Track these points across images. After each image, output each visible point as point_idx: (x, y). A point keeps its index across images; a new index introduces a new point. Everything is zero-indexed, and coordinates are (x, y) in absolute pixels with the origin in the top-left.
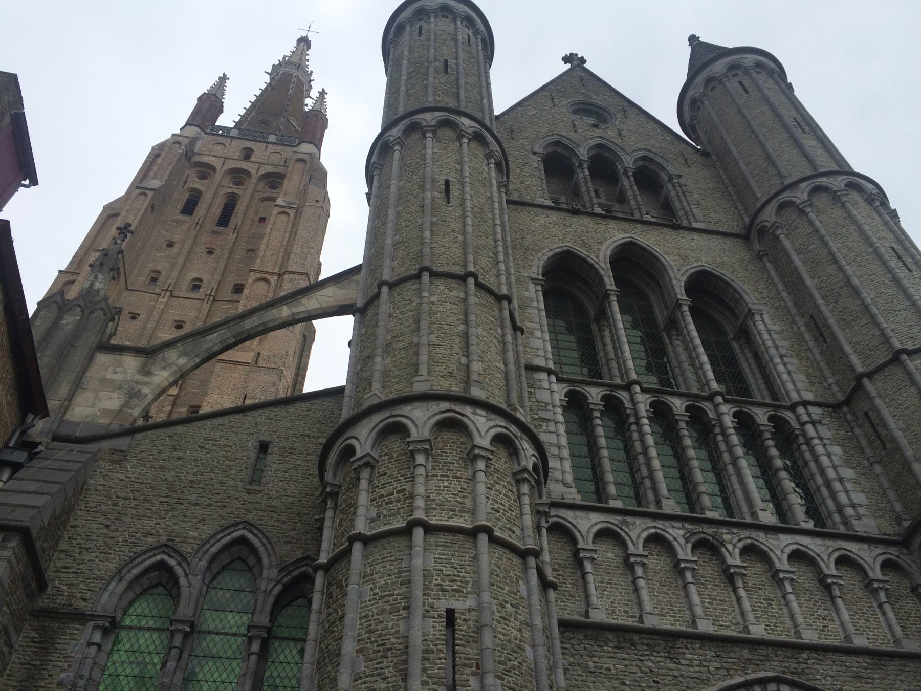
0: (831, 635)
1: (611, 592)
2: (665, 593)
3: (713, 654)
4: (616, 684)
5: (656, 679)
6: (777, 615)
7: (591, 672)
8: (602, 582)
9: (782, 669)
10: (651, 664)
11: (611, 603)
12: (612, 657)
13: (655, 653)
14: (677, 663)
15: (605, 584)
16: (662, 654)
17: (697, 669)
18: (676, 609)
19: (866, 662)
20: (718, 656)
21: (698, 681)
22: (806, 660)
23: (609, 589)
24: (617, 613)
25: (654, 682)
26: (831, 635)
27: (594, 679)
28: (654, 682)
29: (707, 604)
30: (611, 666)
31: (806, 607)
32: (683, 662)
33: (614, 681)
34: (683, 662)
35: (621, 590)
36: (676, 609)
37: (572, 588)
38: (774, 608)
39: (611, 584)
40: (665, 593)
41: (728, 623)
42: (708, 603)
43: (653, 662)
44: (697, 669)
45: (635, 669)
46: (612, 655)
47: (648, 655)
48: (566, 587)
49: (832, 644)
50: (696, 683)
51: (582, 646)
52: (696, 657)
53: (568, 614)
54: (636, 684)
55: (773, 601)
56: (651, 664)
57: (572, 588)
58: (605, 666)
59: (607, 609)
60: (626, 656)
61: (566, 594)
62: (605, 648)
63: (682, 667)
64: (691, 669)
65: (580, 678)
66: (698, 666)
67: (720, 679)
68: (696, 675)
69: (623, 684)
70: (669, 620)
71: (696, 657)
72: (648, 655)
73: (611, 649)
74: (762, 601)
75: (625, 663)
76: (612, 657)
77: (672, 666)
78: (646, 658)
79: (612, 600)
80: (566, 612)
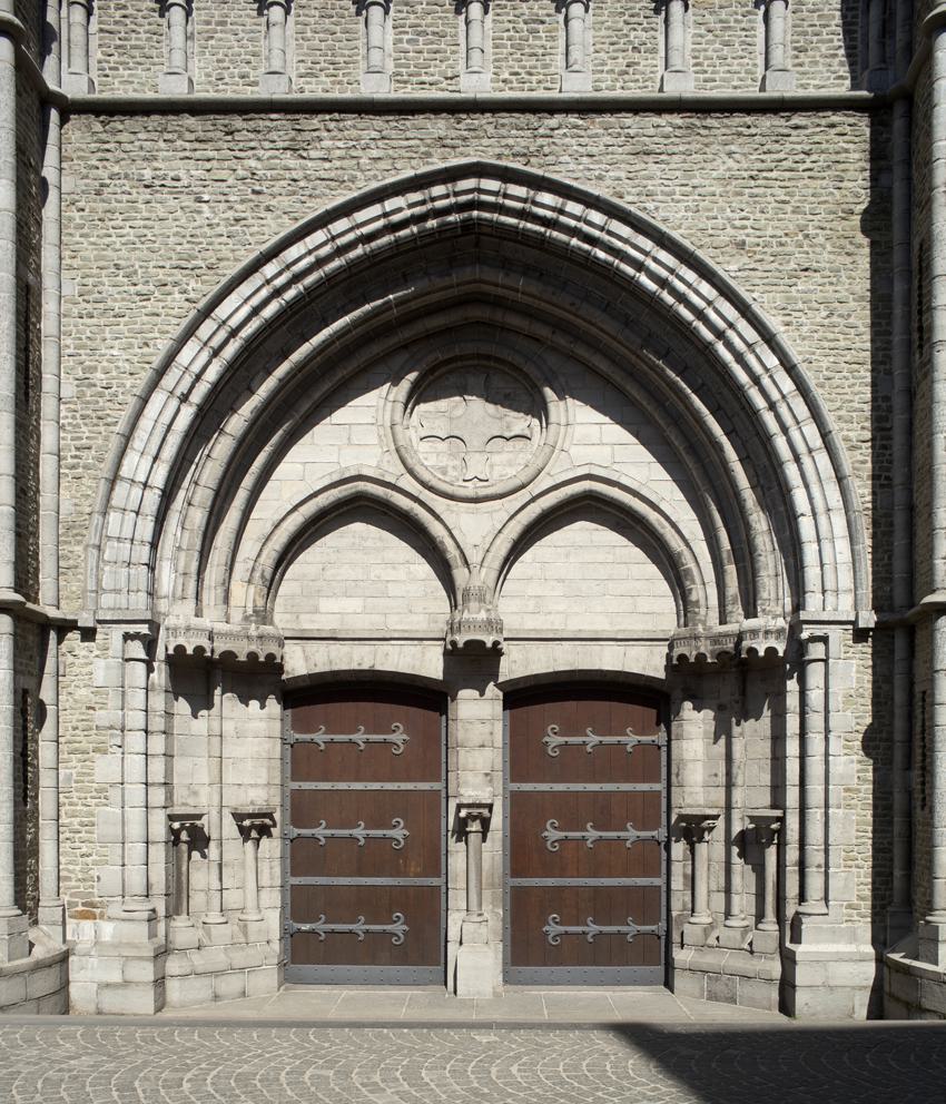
0: (637, 81)
1: (221, 39)
2: (326, 31)
3: (374, 134)
4: (188, 201)
5: (257, 188)
6: (541, 51)
7: (146, 186)
8: (208, 23)
9: (498, 151)
10: (253, 163)
11: (218, 61)
12: (188, 158)
13: (267, 145)
14: (304, 158)
15: (213, 26)
16: (281, 145)
17: (338, 164)
18: (341, 60)
19: (671, 125)
20: (383, 138)
21: (333, 184)
22: (552, 129)
23: (219, 35)
24: (227, 80)
25: (254, 192)
26: (637, 81)
27: (149, 197)
28: (254, 192)
29: (405, 45)
30: (182, 174)
31: (608, 28)
32: (313, 154)
33: (183, 197)
34: (313, 154)
35: (241, 35)
36: (341, 60)
37: (148, 39)
38: (540, 38)
39: (223, 23)
40: (326, 31)
41: (436, 78)
42: (409, 41)
43: (259, 159)
44: (338, 164)
45: (223, 174)
46: (187, 154)
47: (253, 149)
48: (137, 39)
49: (635, 96)
50: (328, 187)
51: (137, 143)
52: (340, 144)
53: (135, 90)
54: (223, 198)
55: (543, 22)
56: (253, 163)
57: (148, 39)
58: (172, 174)
59: (208, 75)
60: (211, 154)
61: (136, 53)
62: (179, 143)
63: (310, 164)
64: (327, 165)
65: (125, 197)
66: (340, 158)
67: (375, 177)
68: (332, 174)
69: (199, 200)
70: (322, 83)
71: (340, 144)
72: (253, 149)
73: (187, 145)
74: (522, 25)
75: (208, 165)
76: (188, 158)
77: (292, 163)
78: (250, 153)
79: (220, 56)
80: (130, 87)
